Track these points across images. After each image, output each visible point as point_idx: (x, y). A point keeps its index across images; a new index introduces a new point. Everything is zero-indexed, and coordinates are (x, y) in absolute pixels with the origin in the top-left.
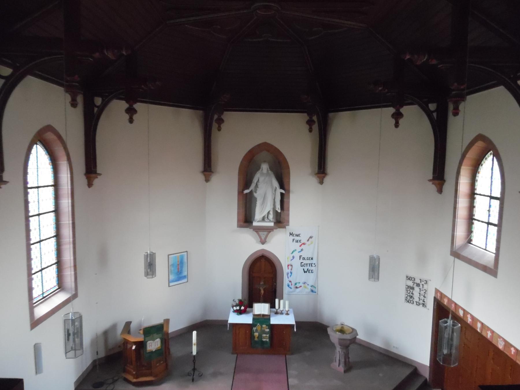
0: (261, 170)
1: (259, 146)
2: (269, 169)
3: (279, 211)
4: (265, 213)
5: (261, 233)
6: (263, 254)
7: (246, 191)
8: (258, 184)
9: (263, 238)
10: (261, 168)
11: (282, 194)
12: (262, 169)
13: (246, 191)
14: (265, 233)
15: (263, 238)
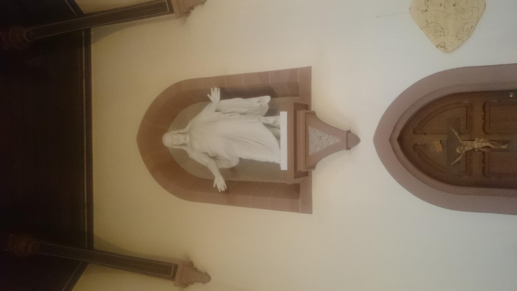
0: (184, 148)
1: (144, 152)
2: (181, 131)
3: (267, 99)
4: (268, 135)
5: (314, 148)
6: (390, 140)
7: (220, 183)
8: (212, 155)
9: (333, 141)
10: (180, 147)
11: (226, 94)
12: (184, 145)
13: (220, 183)
14: (314, 134)
15: (333, 141)
